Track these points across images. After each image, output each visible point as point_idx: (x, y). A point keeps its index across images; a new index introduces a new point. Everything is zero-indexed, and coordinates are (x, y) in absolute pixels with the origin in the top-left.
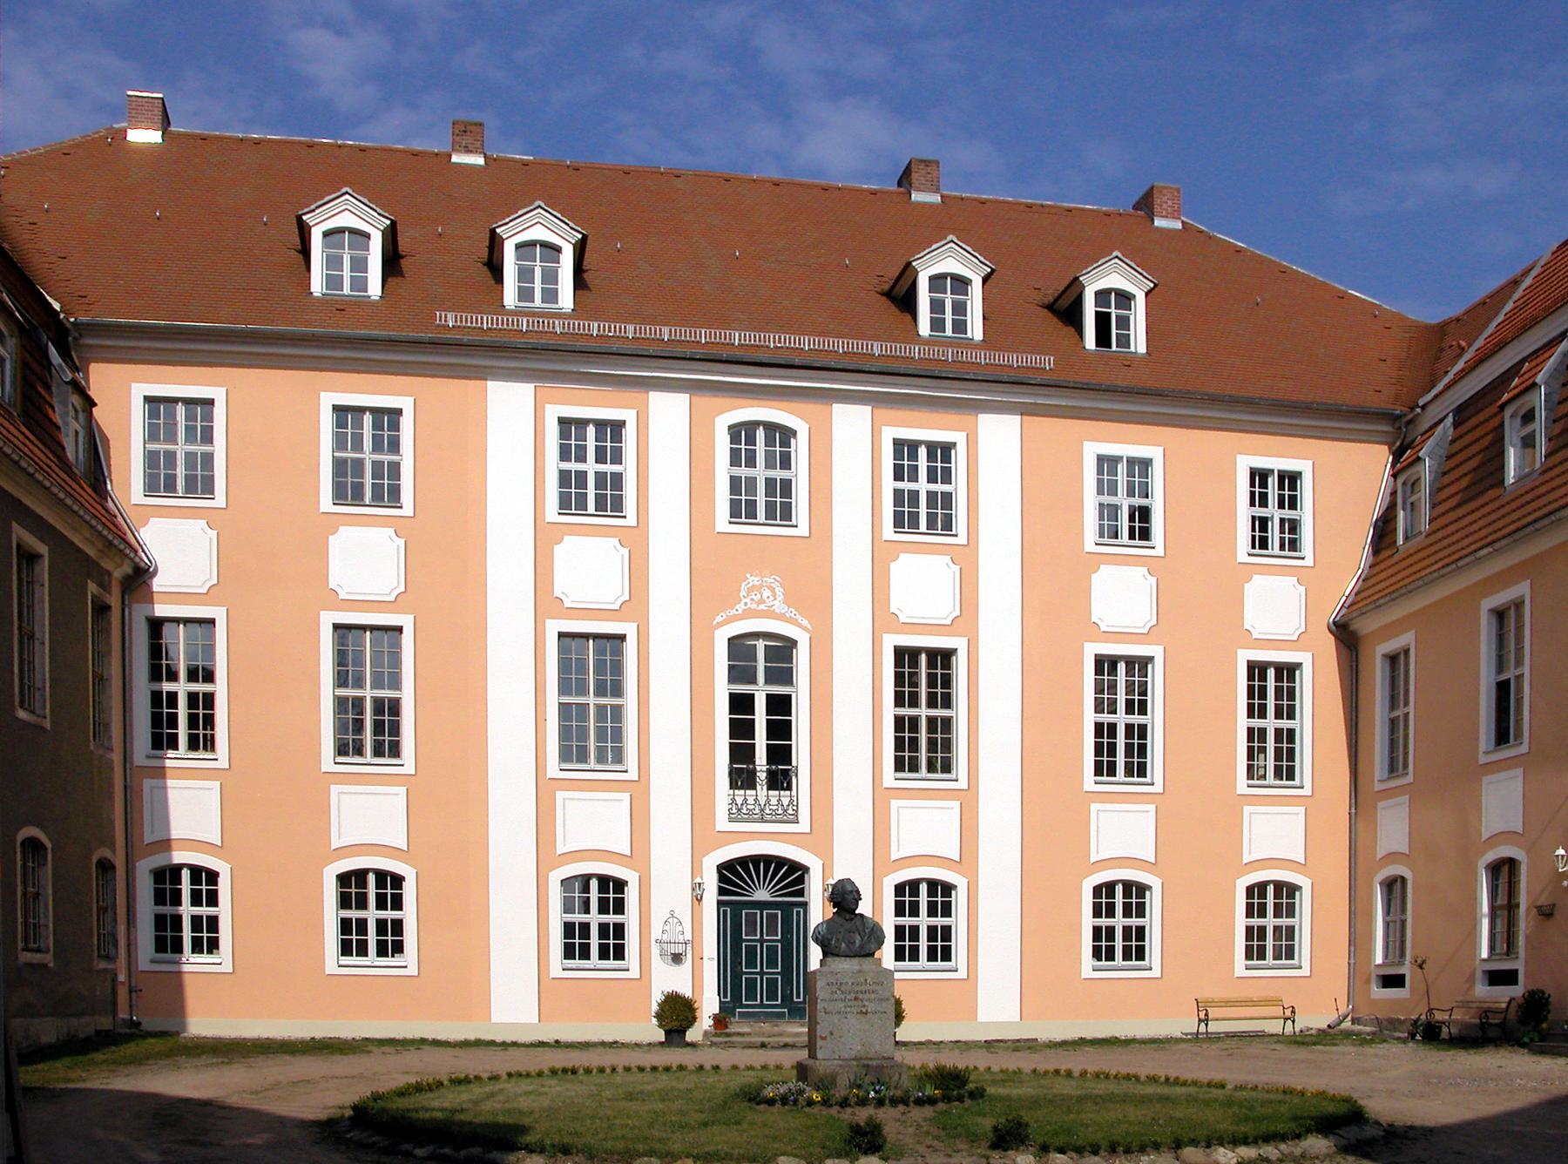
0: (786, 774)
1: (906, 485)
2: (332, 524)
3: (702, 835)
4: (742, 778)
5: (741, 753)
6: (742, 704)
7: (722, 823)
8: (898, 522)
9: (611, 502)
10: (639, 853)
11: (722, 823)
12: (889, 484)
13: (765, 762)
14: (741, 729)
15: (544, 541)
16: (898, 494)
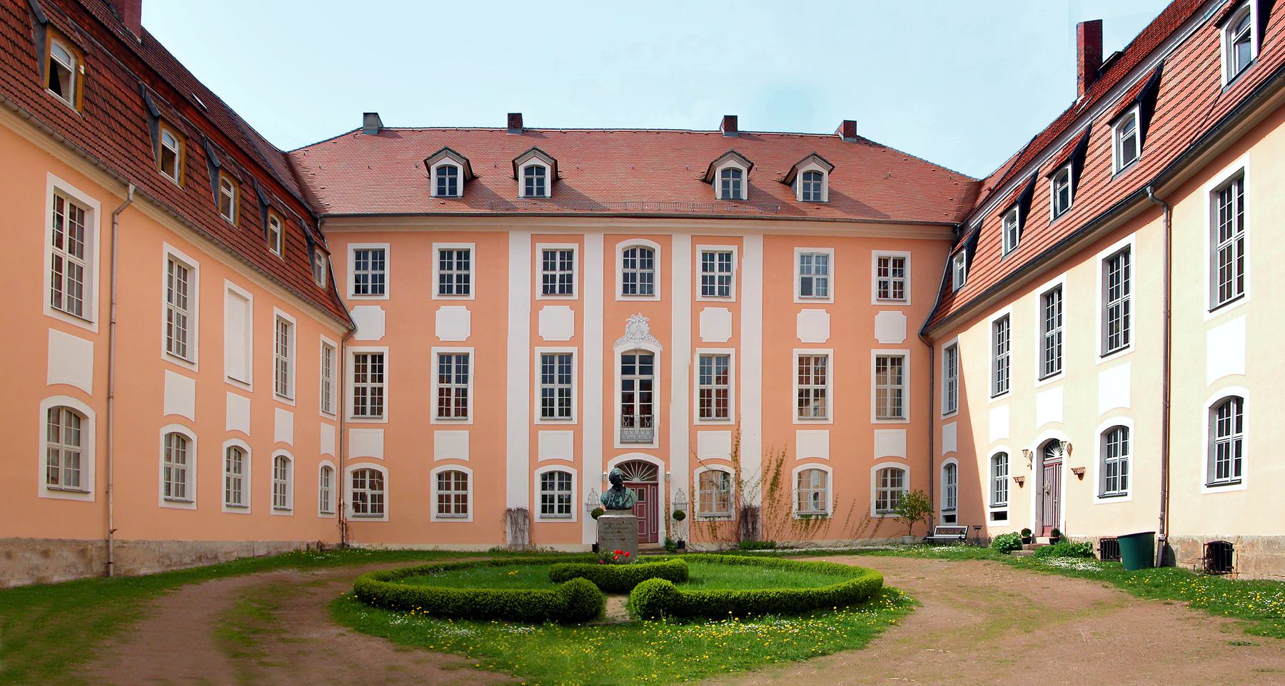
0: (649, 419)
1: (708, 274)
2: (437, 305)
3: (608, 453)
4: (628, 422)
5: (628, 410)
6: (627, 385)
7: (617, 444)
8: (704, 292)
9: (567, 288)
10: (578, 461)
11: (617, 444)
12: (699, 273)
13: (639, 413)
14: (628, 398)
15: (535, 308)
16: (704, 278)
